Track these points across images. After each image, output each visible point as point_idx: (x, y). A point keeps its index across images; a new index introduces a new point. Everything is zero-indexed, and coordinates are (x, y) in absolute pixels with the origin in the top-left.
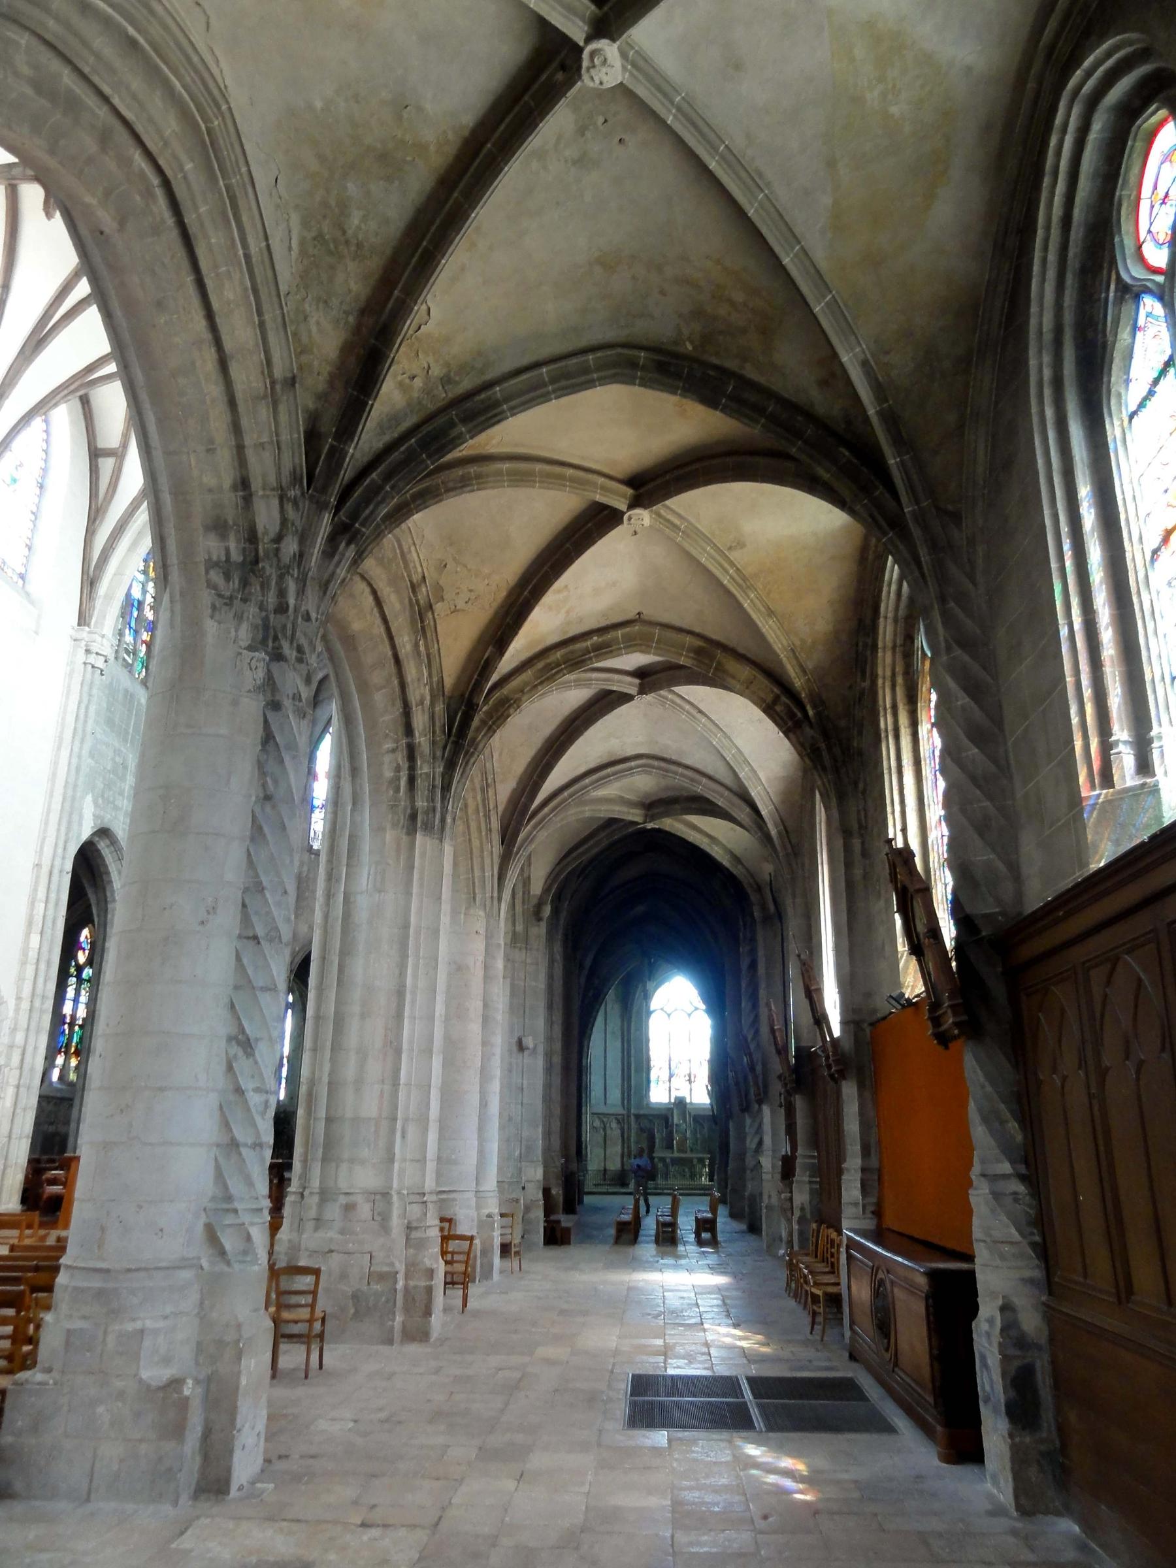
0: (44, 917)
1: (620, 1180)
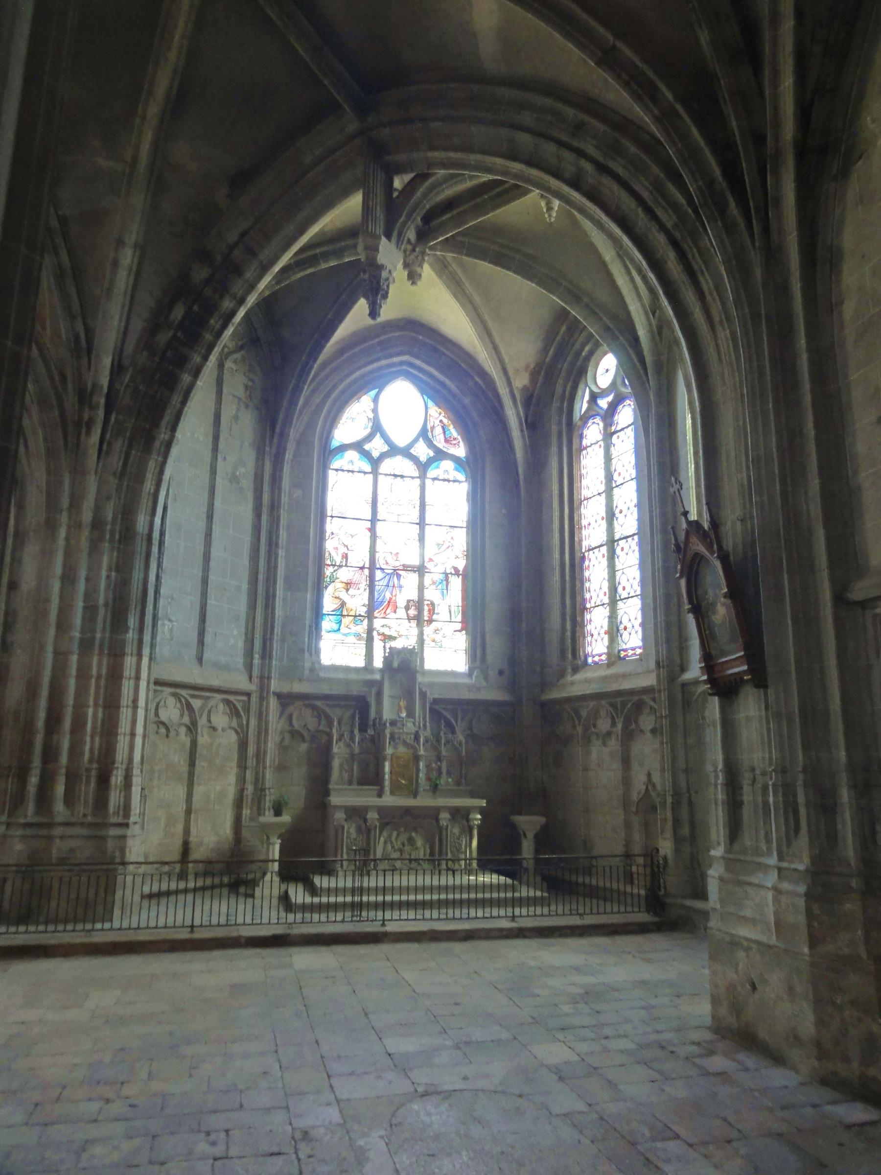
1: (232, 873)
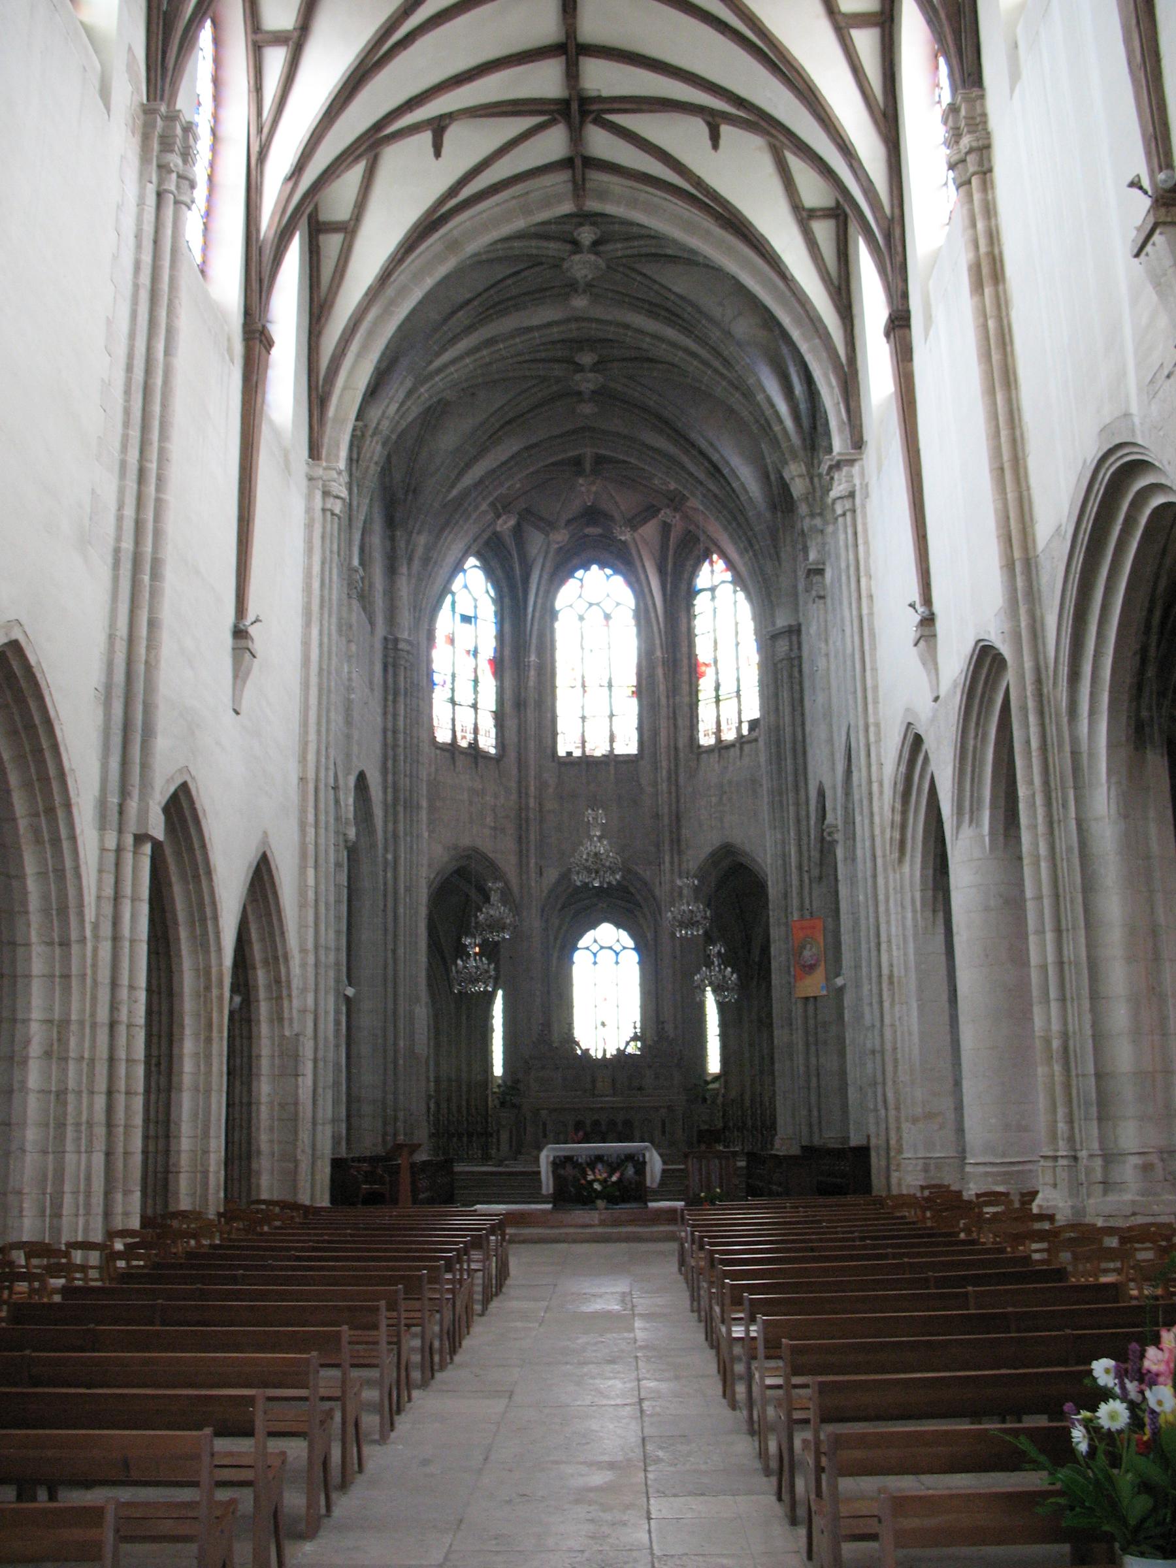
0: (316, 845)
